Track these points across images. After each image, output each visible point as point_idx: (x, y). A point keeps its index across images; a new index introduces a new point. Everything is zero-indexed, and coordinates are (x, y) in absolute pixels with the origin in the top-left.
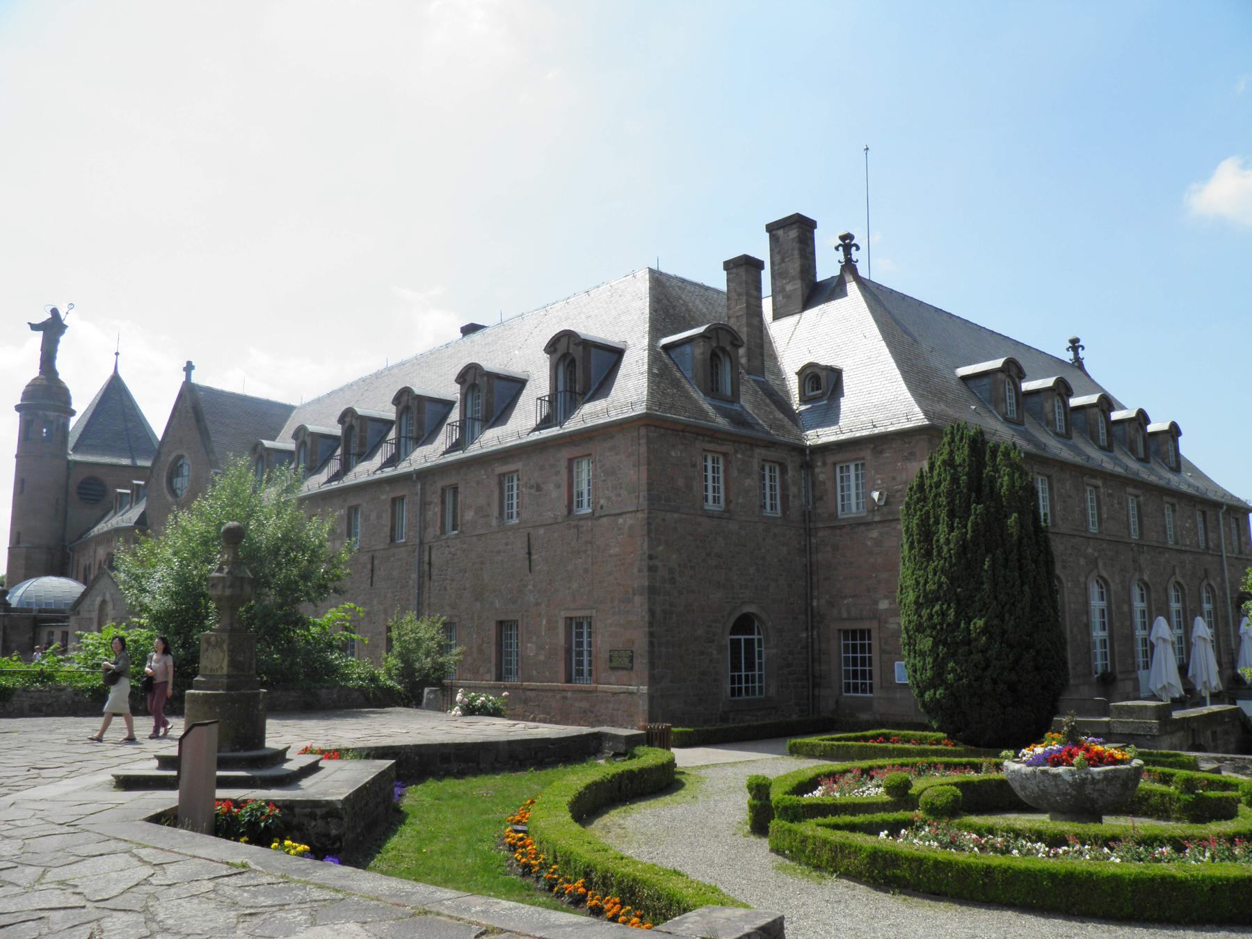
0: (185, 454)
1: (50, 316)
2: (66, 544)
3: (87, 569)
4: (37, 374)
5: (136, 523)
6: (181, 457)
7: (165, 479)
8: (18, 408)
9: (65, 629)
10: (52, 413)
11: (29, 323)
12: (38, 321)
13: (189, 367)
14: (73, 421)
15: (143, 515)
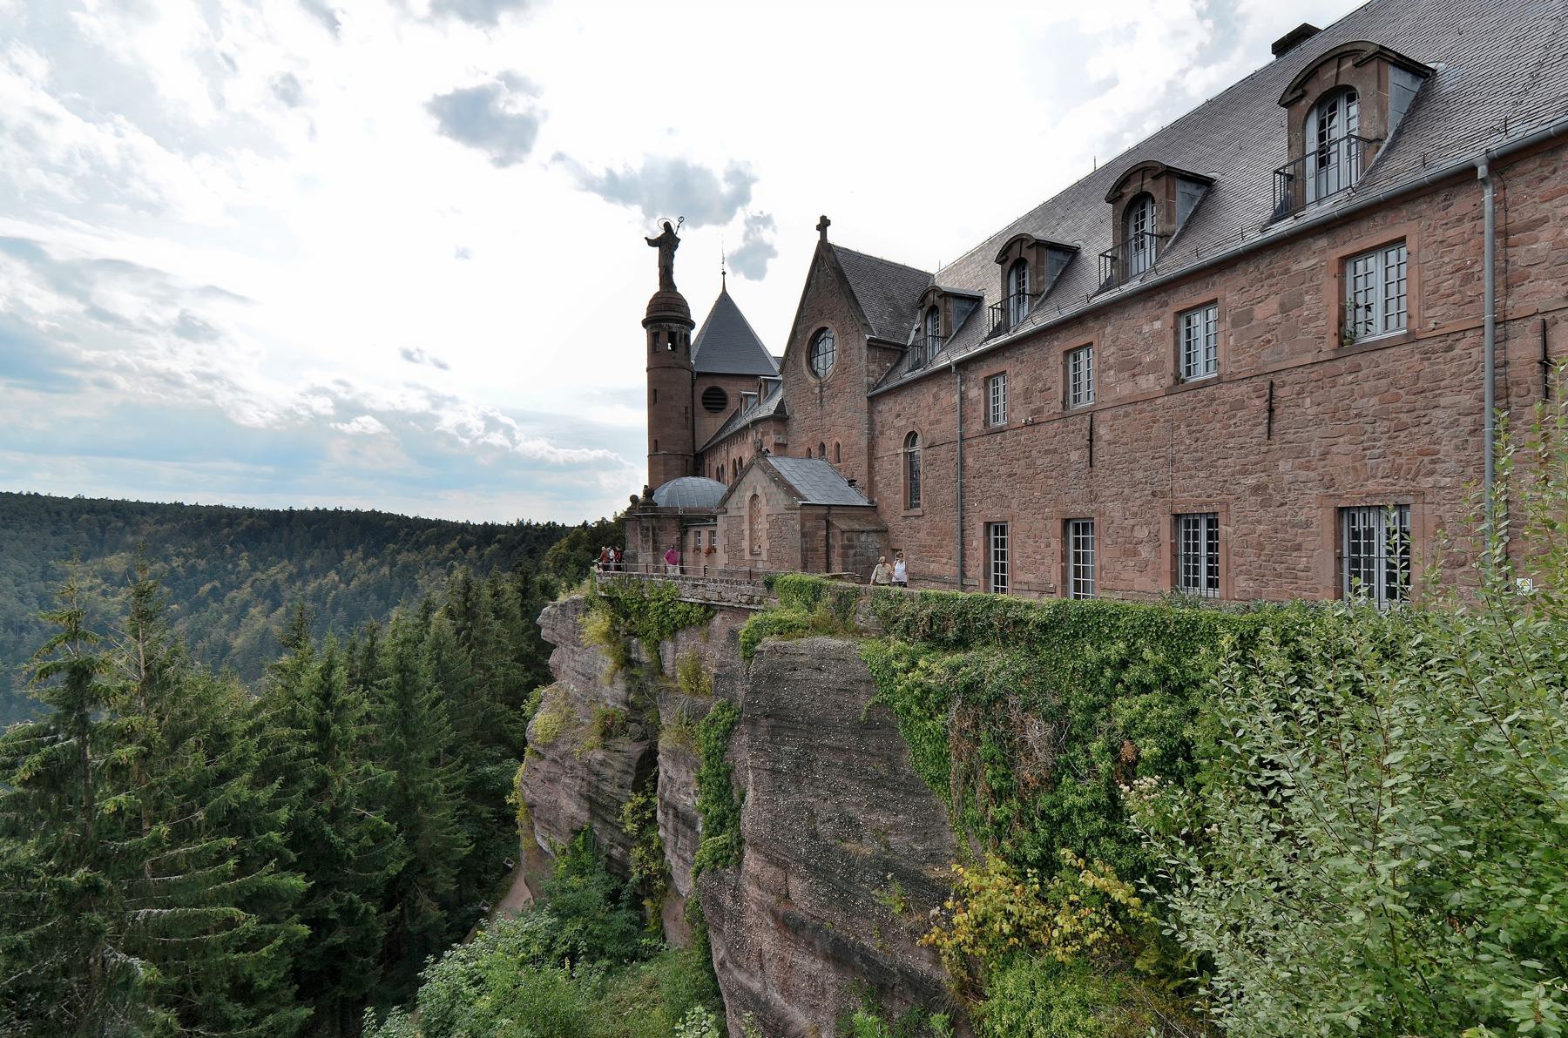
4: (657, 289)
7: (804, 360)
8: (645, 323)
9: (712, 529)
13: (824, 224)
14: (694, 335)
15: (781, 406)
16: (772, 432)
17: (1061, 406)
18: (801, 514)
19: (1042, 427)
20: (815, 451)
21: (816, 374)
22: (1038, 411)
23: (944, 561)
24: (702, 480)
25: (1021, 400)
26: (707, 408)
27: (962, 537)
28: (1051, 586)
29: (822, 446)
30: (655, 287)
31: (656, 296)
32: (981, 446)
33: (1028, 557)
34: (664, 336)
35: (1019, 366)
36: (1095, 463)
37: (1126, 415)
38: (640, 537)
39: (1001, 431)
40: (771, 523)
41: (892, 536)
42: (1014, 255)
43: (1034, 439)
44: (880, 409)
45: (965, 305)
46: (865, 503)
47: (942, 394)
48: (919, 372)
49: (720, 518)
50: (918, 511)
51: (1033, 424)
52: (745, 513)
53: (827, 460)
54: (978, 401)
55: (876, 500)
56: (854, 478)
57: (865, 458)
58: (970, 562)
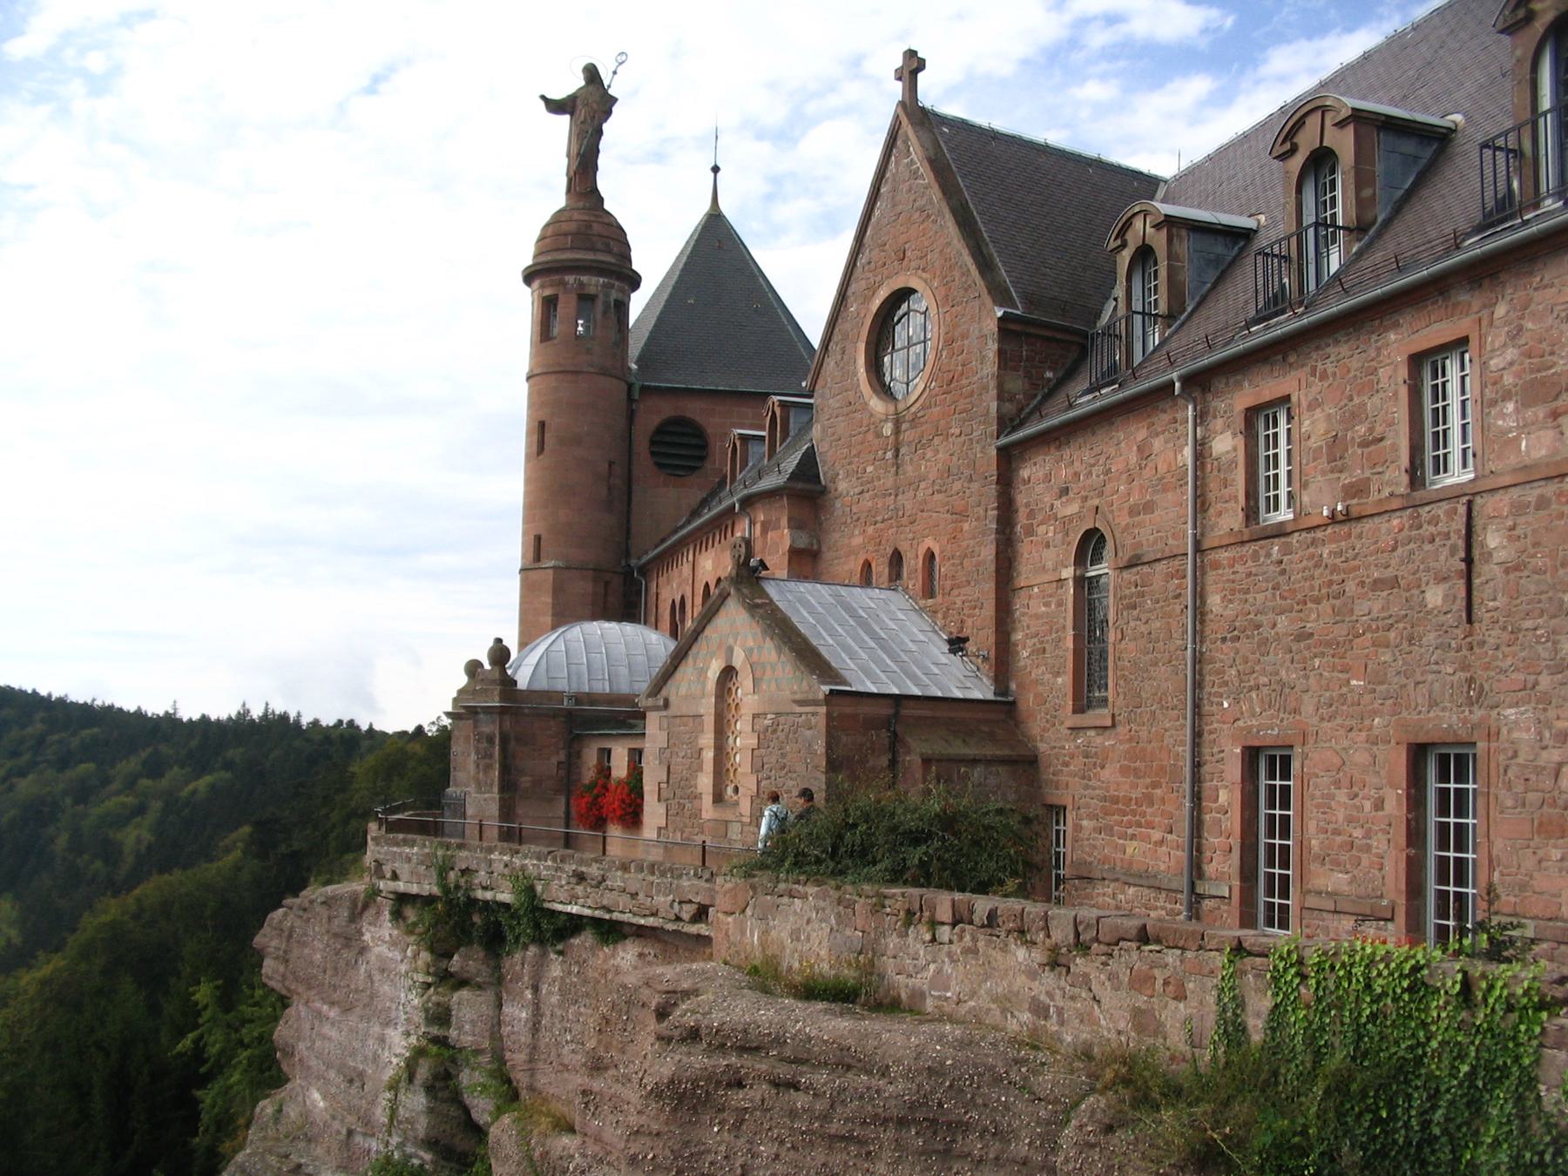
0: (914, 283)
1: (582, 83)
2: (633, 562)
3: (679, 608)
5: (794, 476)
6: (904, 294)
8: (529, 277)
9: (635, 744)
10: (594, 279)
11: (543, 97)
12: (558, 94)
13: (912, 66)
14: (638, 303)
16: (784, 521)
17: (1405, 479)
18: (829, 715)
19: (1367, 525)
20: (881, 569)
21: (885, 390)
22: (1358, 490)
23: (1156, 835)
24: (629, 628)
25: (1323, 463)
26: (657, 464)
27: (1197, 779)
28: (1385, 903)
29: (896, 559)
30: (559, 200)
31: (558, 218)
32: (1238, 567)
33: (1336, 832)
34: (566, 306)
35: (1317, 386)
36: (1479, 612)
37: (1542, 503)
38: (473, 757)
39: (1280, 532)
40: (764, 737)
41: (1047, 775)
42: (1307, 141)
43: (1350, 553)
44: (1025, 473)
45: (1219, 248)
46: (982, 690)
47: (1157, 444)
48: (1110, 396)
49: (653, 719)
50: (1100, 716)
51: (1348, 518)
52: (707, 707)
53: (906, 590)
54: (1234, 462)
55: (1013, 686)
56: (965, 633)
57: (986, 590)
58: (1212, 840)
